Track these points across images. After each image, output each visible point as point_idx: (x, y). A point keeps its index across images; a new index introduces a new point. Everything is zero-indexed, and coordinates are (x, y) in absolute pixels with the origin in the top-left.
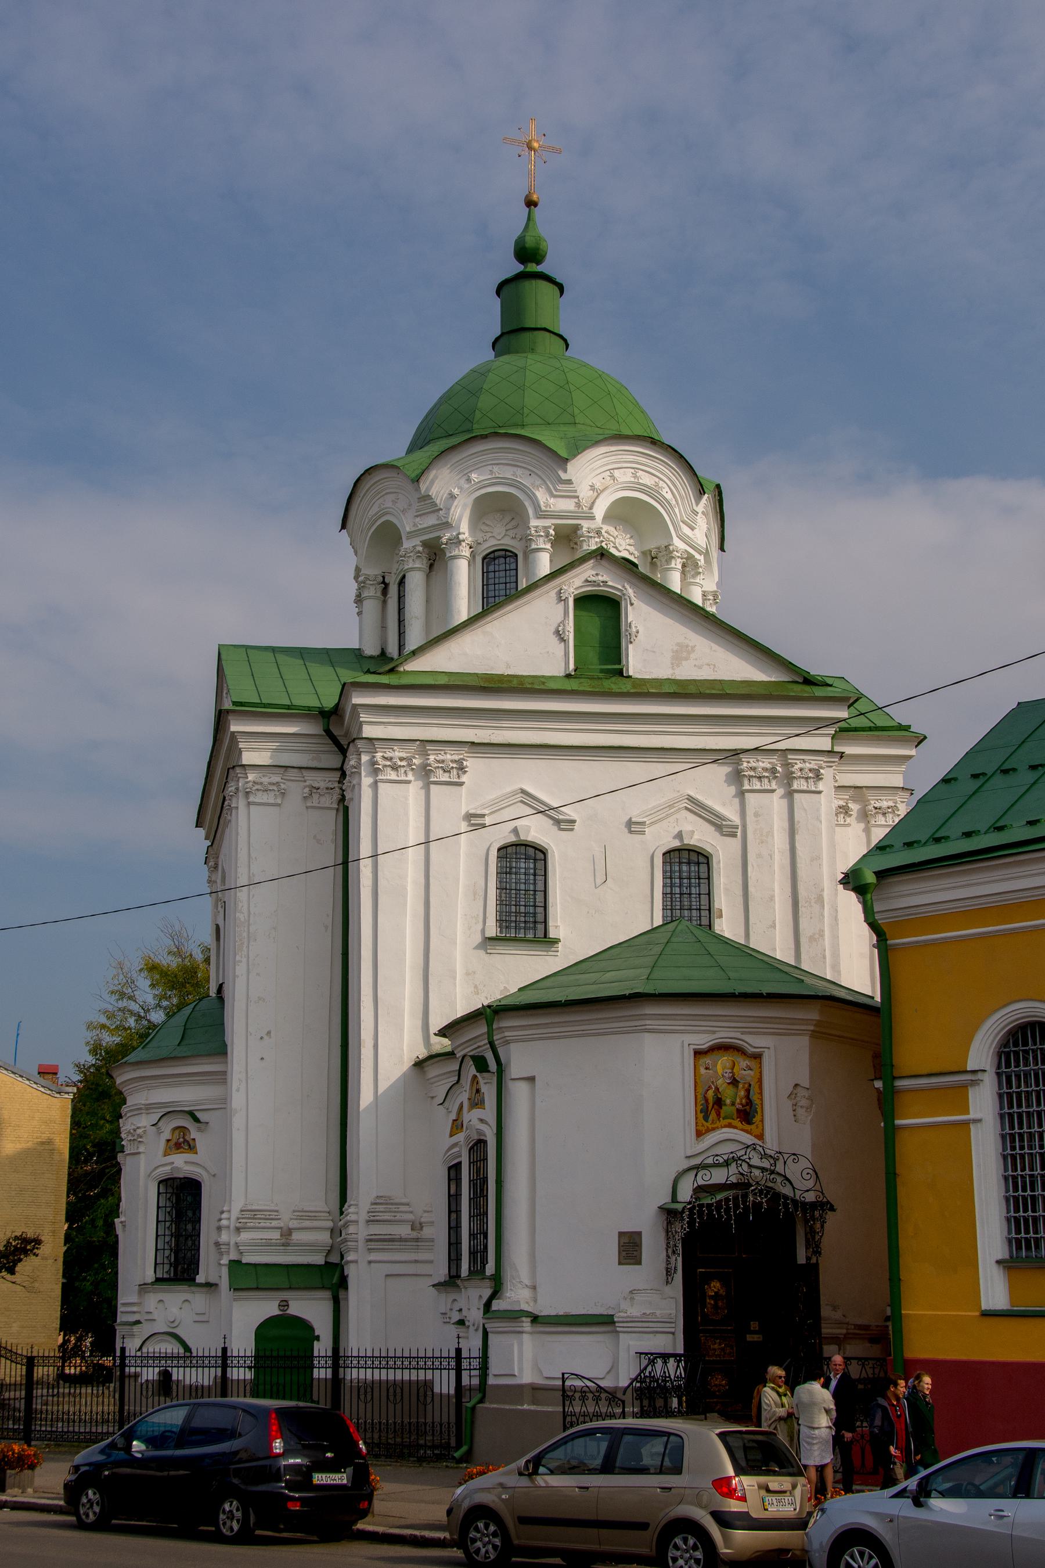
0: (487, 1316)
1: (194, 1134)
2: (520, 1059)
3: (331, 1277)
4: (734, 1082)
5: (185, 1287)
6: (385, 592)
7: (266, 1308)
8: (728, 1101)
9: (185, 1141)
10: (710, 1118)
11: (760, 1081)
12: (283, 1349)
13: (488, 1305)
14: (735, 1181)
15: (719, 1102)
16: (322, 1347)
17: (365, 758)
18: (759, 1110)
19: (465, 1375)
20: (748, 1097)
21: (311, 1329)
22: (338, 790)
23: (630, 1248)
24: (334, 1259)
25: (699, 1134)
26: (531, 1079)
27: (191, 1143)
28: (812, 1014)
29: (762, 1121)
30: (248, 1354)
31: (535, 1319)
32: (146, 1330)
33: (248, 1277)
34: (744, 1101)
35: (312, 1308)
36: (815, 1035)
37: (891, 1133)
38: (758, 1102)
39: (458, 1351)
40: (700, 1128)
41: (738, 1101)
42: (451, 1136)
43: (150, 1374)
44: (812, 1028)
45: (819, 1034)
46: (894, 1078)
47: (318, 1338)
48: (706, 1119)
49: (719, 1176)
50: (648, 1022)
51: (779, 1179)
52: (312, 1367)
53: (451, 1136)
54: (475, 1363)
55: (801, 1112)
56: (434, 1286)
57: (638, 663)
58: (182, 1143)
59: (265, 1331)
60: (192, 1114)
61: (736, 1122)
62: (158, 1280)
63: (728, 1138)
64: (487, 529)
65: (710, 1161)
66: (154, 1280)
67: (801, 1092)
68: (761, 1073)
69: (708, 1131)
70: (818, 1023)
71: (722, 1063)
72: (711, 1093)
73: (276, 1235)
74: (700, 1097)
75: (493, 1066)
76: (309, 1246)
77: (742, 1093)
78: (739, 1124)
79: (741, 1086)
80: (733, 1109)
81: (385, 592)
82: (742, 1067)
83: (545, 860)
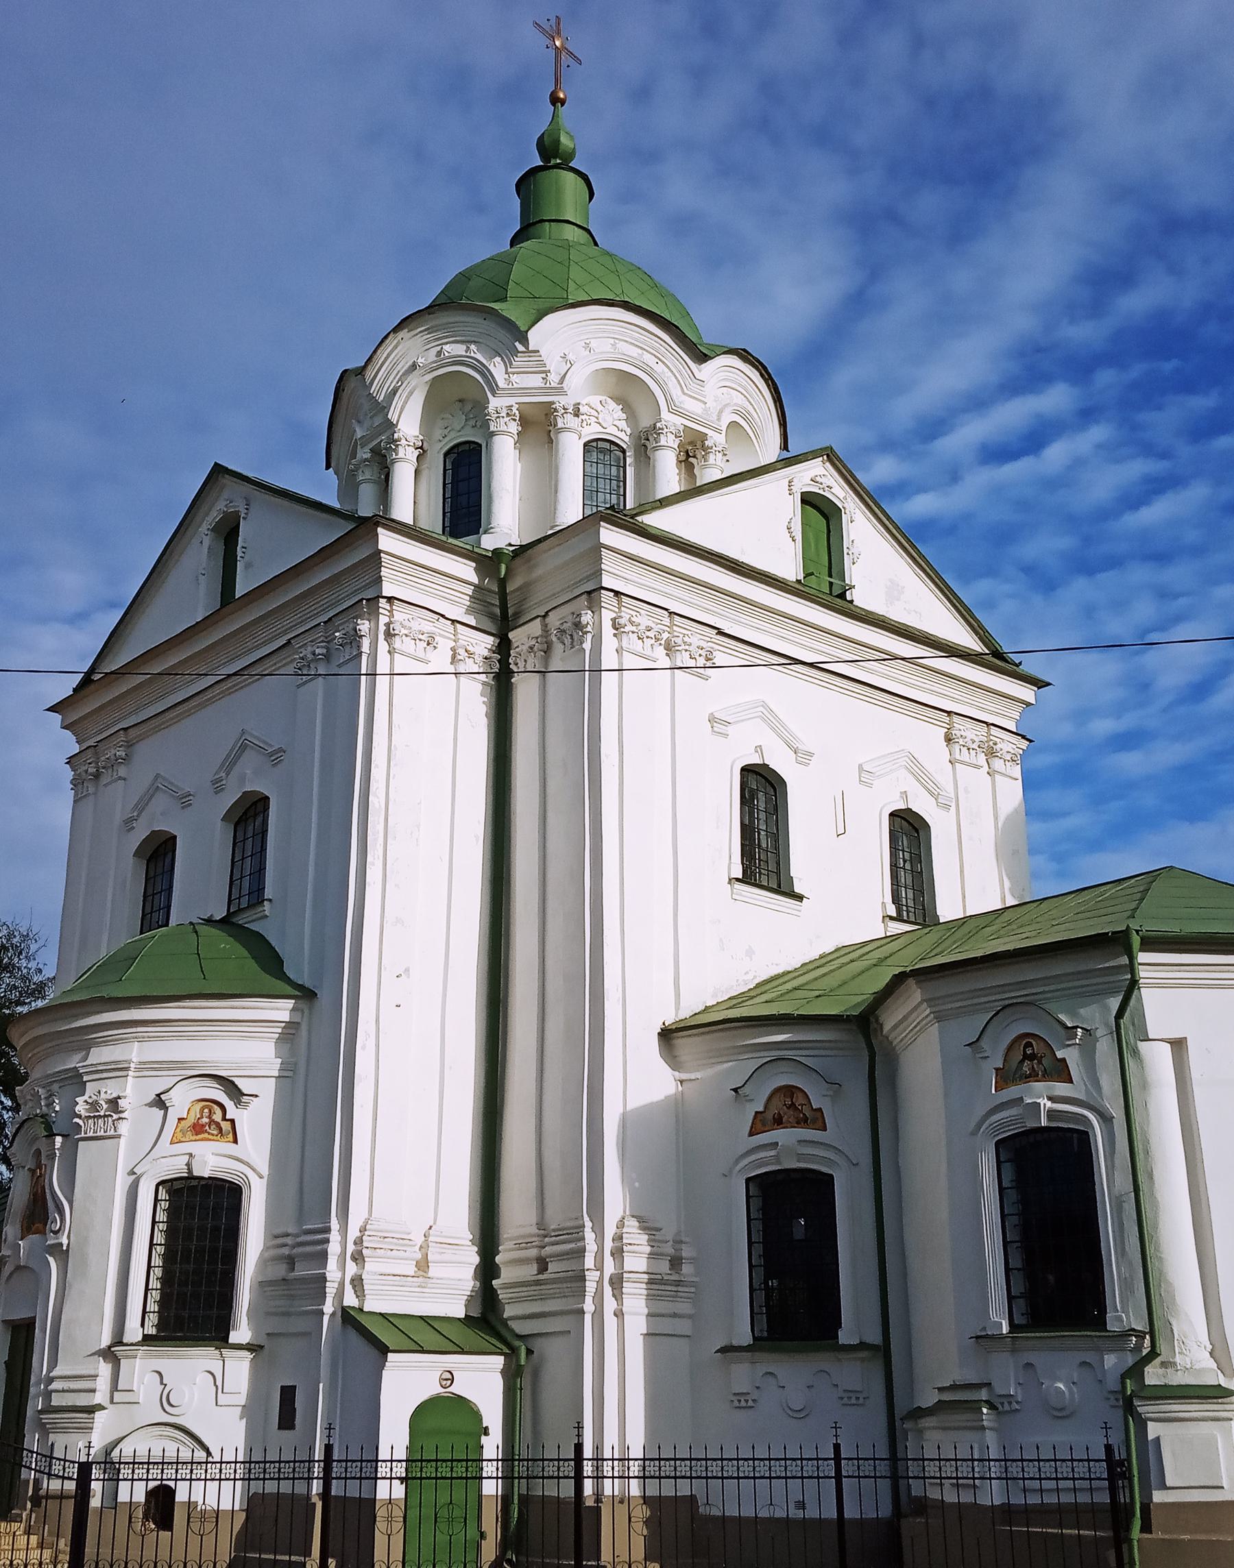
1: (232, 1112)
5: (211, 1351)
9: (212, 1121)
16: (492, 1445)
17: (607, 616)
27: (226, 1126)
42: (751, 1134)
43: (133, 1492)
53: (751, 1134)
60: (228, 1084)
62: (147, 1339)
66: (140, 1338)
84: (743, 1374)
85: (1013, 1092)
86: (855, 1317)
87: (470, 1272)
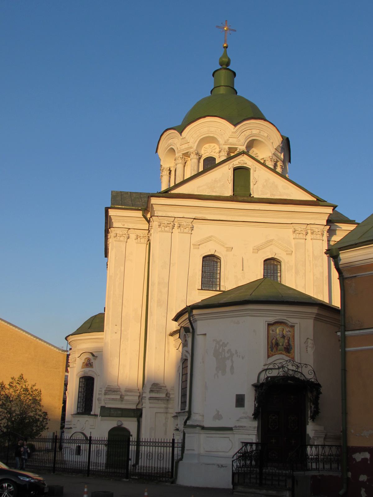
0: (185, 426)
2: (201, 327)
3: (137, 414)
4: (283, 337)
5: (87, 416)
6: (170, 173)
7: (112, 423)
8: (281, 344)
9: (90, 363)
10: (274, 351)
11: (294, 336)
12: (119, 440)
13: (185, 422)
14: (282, 375)
15: (277, 344)
16: (134, 438)
18: (293, 348)
19: (176, 449)
20: (289, 342)
21: (129, 432)
22: (147, 237)
23: (240, 401)
24: (139, 407)
25: (269, 357)
26: (205, 334)
27: (91, 364)
28: (315, 310)
29: (294, 352)
30: (105, 439)
31: (203, 428)
32: (73, 431)
33: (106, 412)
34: (287, 344)
36: (316, 319)
37: (344, 354)
38: (292, 345)
39: (173, 440)
40: (269, 354)
41: (285, 344)
44: (314, 316)
45: (317, 318)
46: (345, 331)
47: (132, 436)
48: (272, 351)
49: (275, 373)
50: (250, 312)
51: (299, 374)
52: (129, 445)
54: (180, 445)
55: (309, 349)
56: (173, 417)
57: (256, 191)
59: (112, 432)
61: (284, 352)
63: (280, 358)
64: (206, 149)
65: (271, 366)
66: (77, 413)
67: (310, 341)
68: (294, 333)
69: (273, 355)
70: (318, 314)
71: (278, 330)
72: (274, 341)
73: (119, 397)
74: (270, 342)
75: (191, 330)
77: (286, 341)
78: (285, 353)
79: (286, 338)
80: (283, 347)
81: (170, 173)
82: (286, 331)
83: (220, 262)
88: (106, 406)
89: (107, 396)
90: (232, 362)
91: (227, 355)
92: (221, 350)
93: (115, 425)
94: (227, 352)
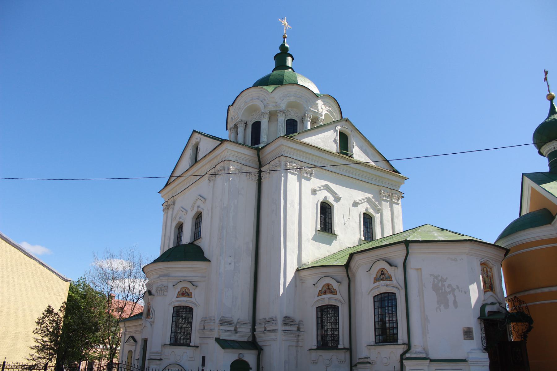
9: (186, 293)
23: (468, 333)
24: (251, 340)
26: (419, 270)
31: (431, 361)
35: (250, 357)
42: (318, 296)
47: (251, 369)
53: (318, 296)
58: (185, 293)
76: (244, 334)
84: (315, 355)
85: (377, 284)
86: (344, 342)
87: (249, 330)
88: (221, 338)
89: (222, 328)
90: (455, 296)
91: (448, 290)
92: (440, 285)
93: (237, 358)
94: (448, 287)
